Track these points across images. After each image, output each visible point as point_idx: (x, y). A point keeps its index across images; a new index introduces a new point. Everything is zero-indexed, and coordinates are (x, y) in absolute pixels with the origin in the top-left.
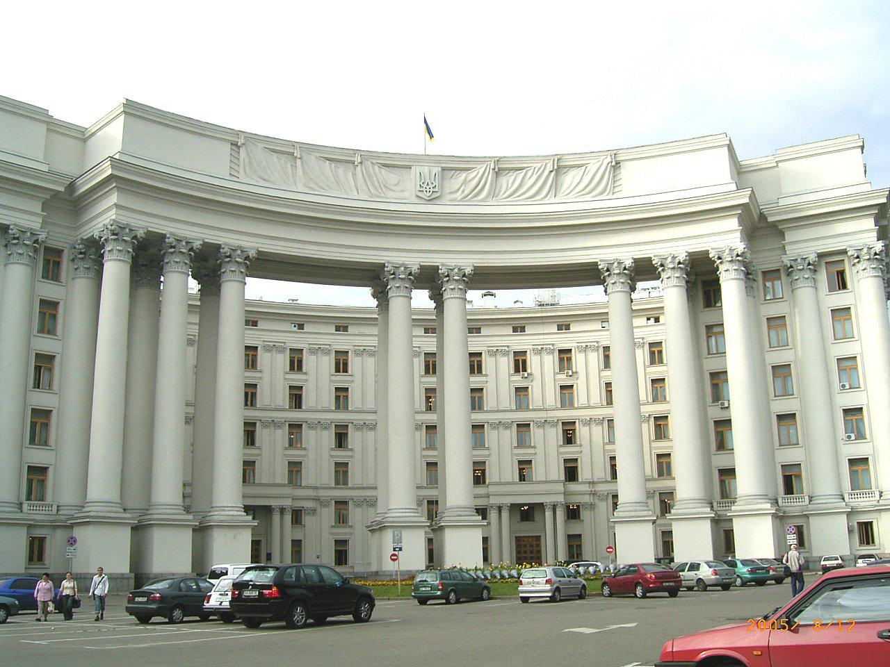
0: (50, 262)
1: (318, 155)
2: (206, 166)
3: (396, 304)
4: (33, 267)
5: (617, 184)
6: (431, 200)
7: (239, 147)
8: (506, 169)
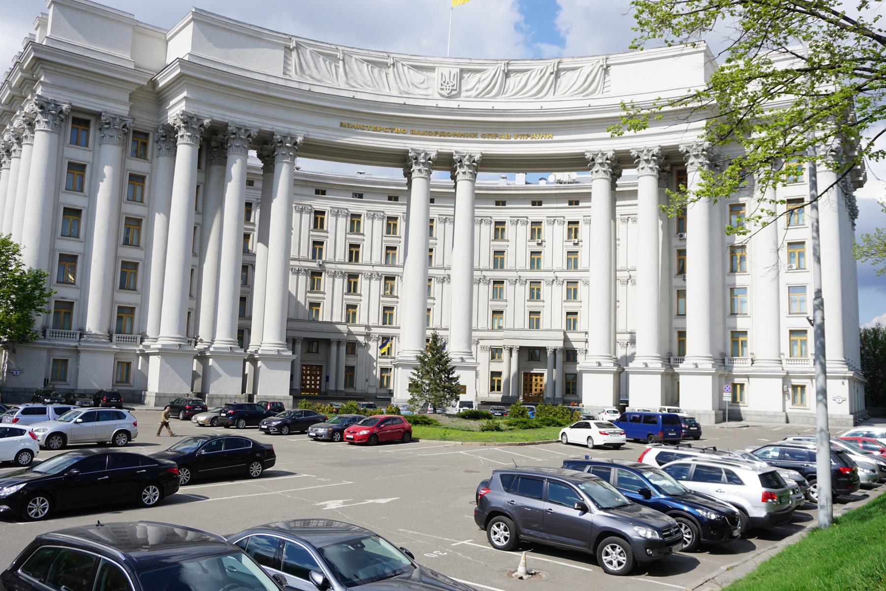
1: (357, 57)
3: (418, 184)
4: (124, 145)
5: (606, 85)
6: (450, 97)
7: (291, 50)
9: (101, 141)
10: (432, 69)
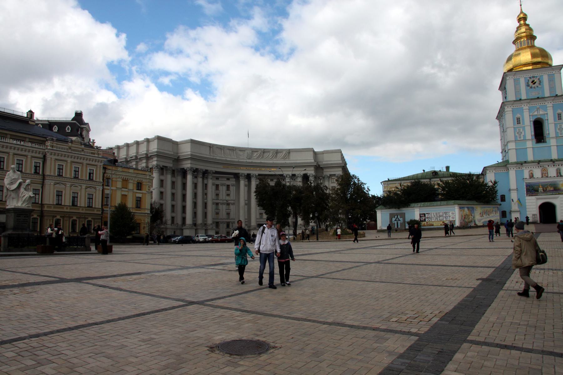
0: (173, 172)
2: (205, 153)
6: (249, 159)
9: (167, 174)
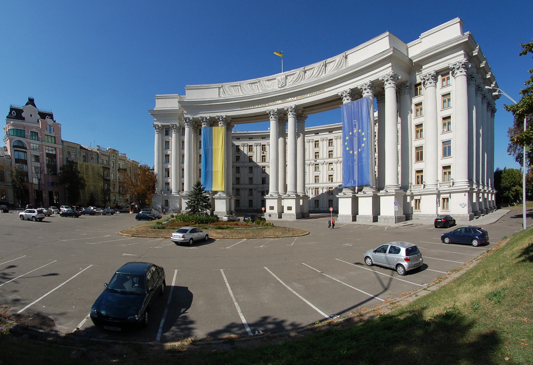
8: (307, 70)
10: (275, 79)
